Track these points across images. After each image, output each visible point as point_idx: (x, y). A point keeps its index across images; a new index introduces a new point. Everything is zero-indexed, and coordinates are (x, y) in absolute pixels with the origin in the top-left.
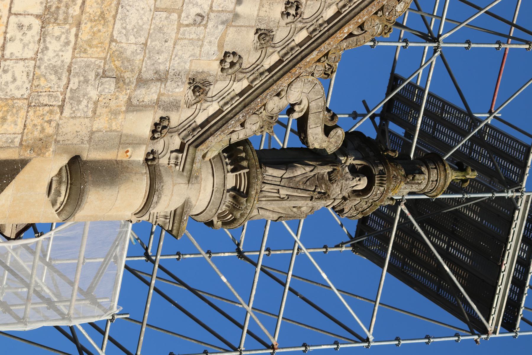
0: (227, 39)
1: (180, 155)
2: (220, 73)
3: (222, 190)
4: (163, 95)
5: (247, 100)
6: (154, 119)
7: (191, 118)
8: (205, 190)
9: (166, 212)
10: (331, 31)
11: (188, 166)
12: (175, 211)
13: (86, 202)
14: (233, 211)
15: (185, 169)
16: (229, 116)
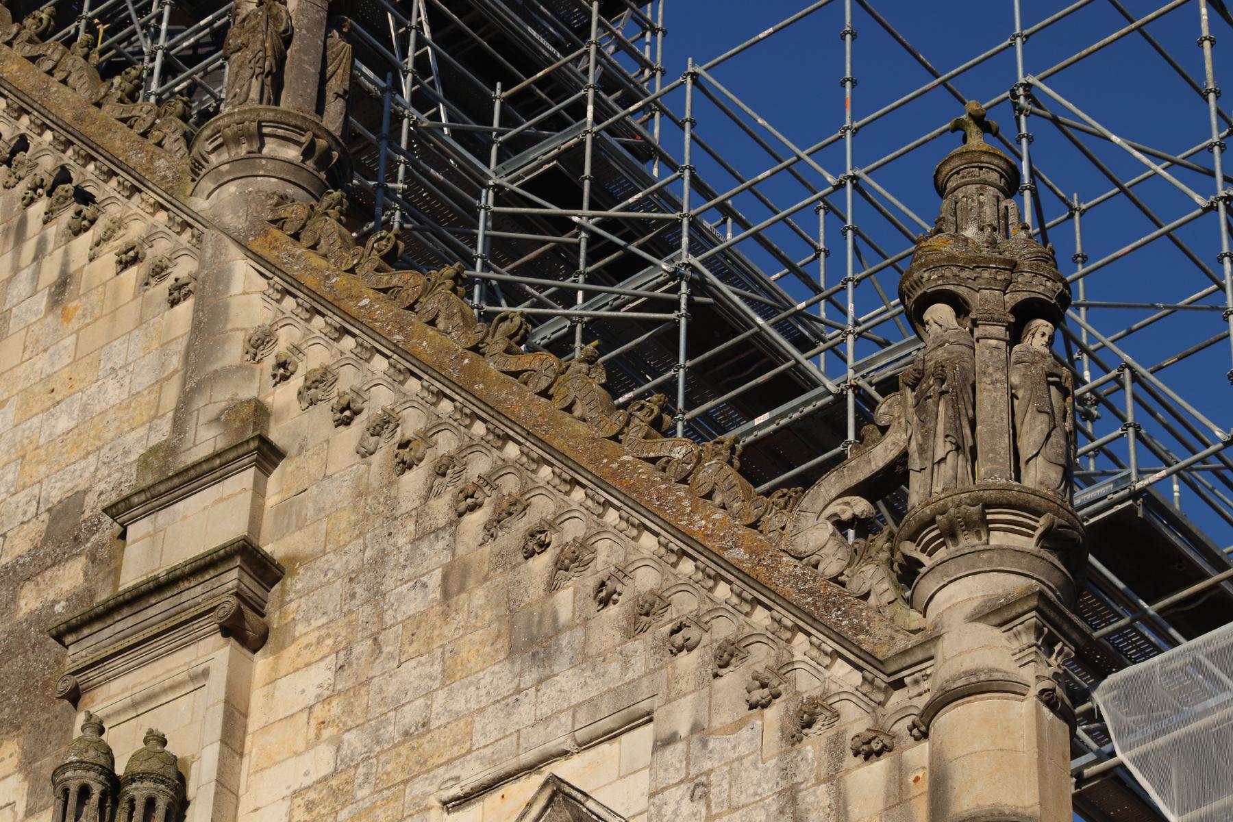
0: (729, 721)
1: (907, 680)
2: (783, 697)
3: (939, 568)
4: (817, 777)
5: (810, 621)
6: (859, 766)
7: (854, 699)
8: (951, 597)
9: (1009, 639)
10: (701, 549)
11: (920, 655)
12: (1000, 625)
13: (978, 806)
14: (975, 522)
15: (927, 655)
16: (833, 636)
